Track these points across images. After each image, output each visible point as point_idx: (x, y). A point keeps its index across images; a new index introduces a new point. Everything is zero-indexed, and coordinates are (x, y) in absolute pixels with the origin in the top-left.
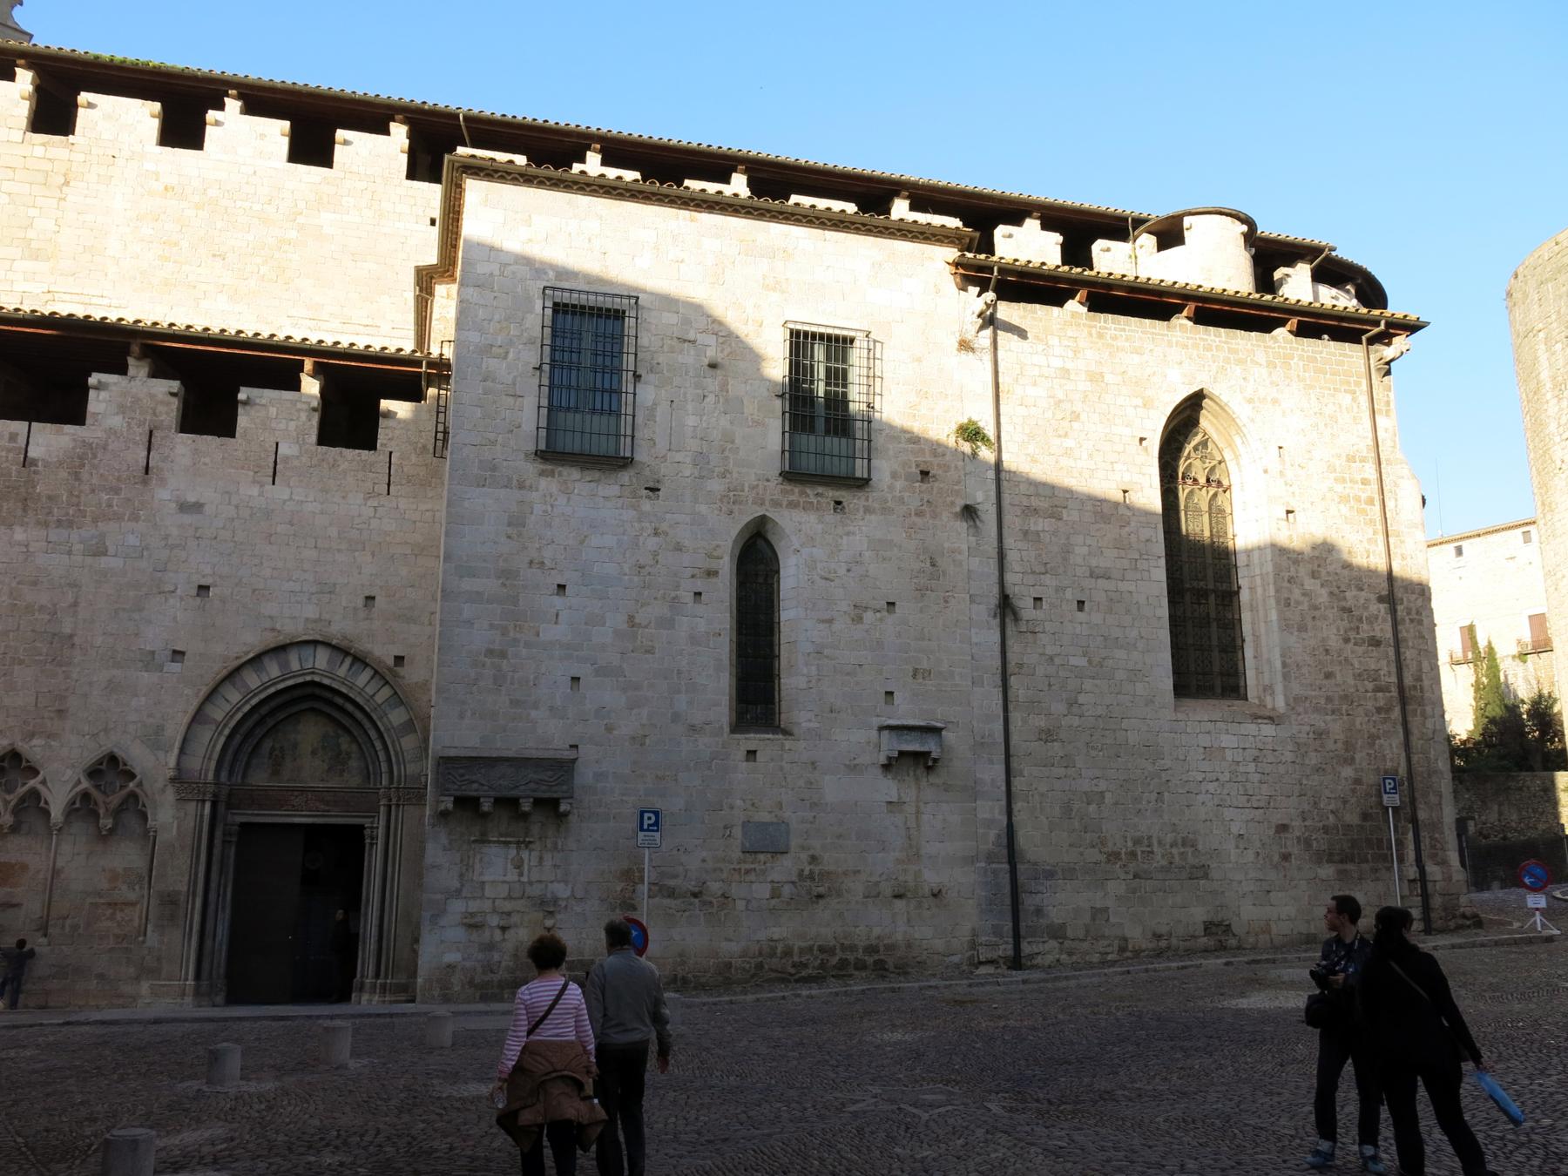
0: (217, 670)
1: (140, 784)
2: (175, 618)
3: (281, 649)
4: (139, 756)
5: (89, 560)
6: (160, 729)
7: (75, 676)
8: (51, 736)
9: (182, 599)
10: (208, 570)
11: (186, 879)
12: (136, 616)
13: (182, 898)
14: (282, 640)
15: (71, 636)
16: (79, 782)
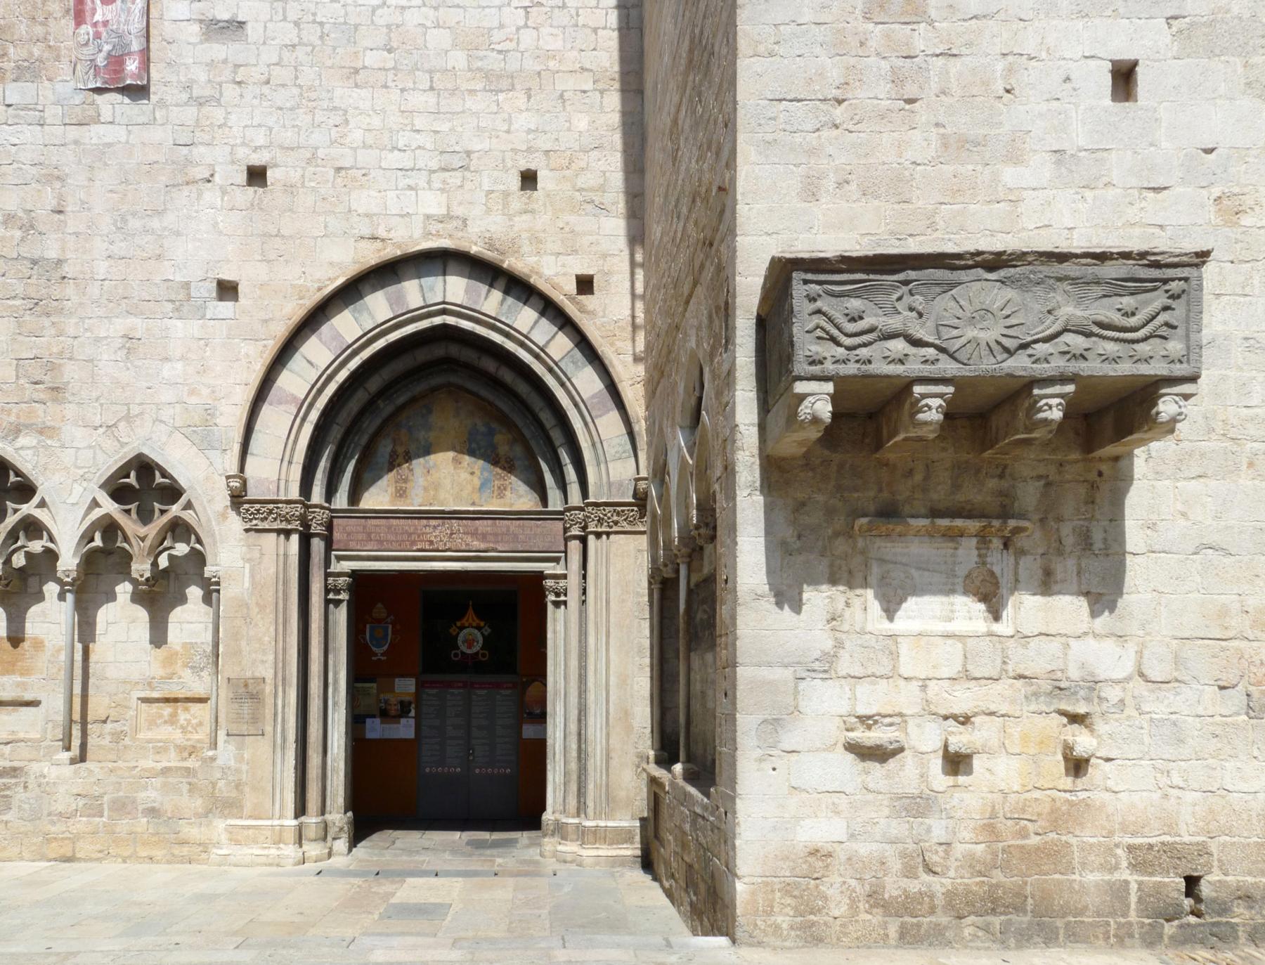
0: (295, 310)
1: (189, 506)
2: (215, 225)
3: (387, 272)
4: (180, 460)
5: (73, 132)
6: (210, 412)
7: (71, 331)
8: (43, 431)
9: (224, 192)
10: (261, 141)
11: (271, 657)
12: (155, 223)
13: (268, 689)
14: (390, 252)
15: (59, 262)
16: (95, 504)
